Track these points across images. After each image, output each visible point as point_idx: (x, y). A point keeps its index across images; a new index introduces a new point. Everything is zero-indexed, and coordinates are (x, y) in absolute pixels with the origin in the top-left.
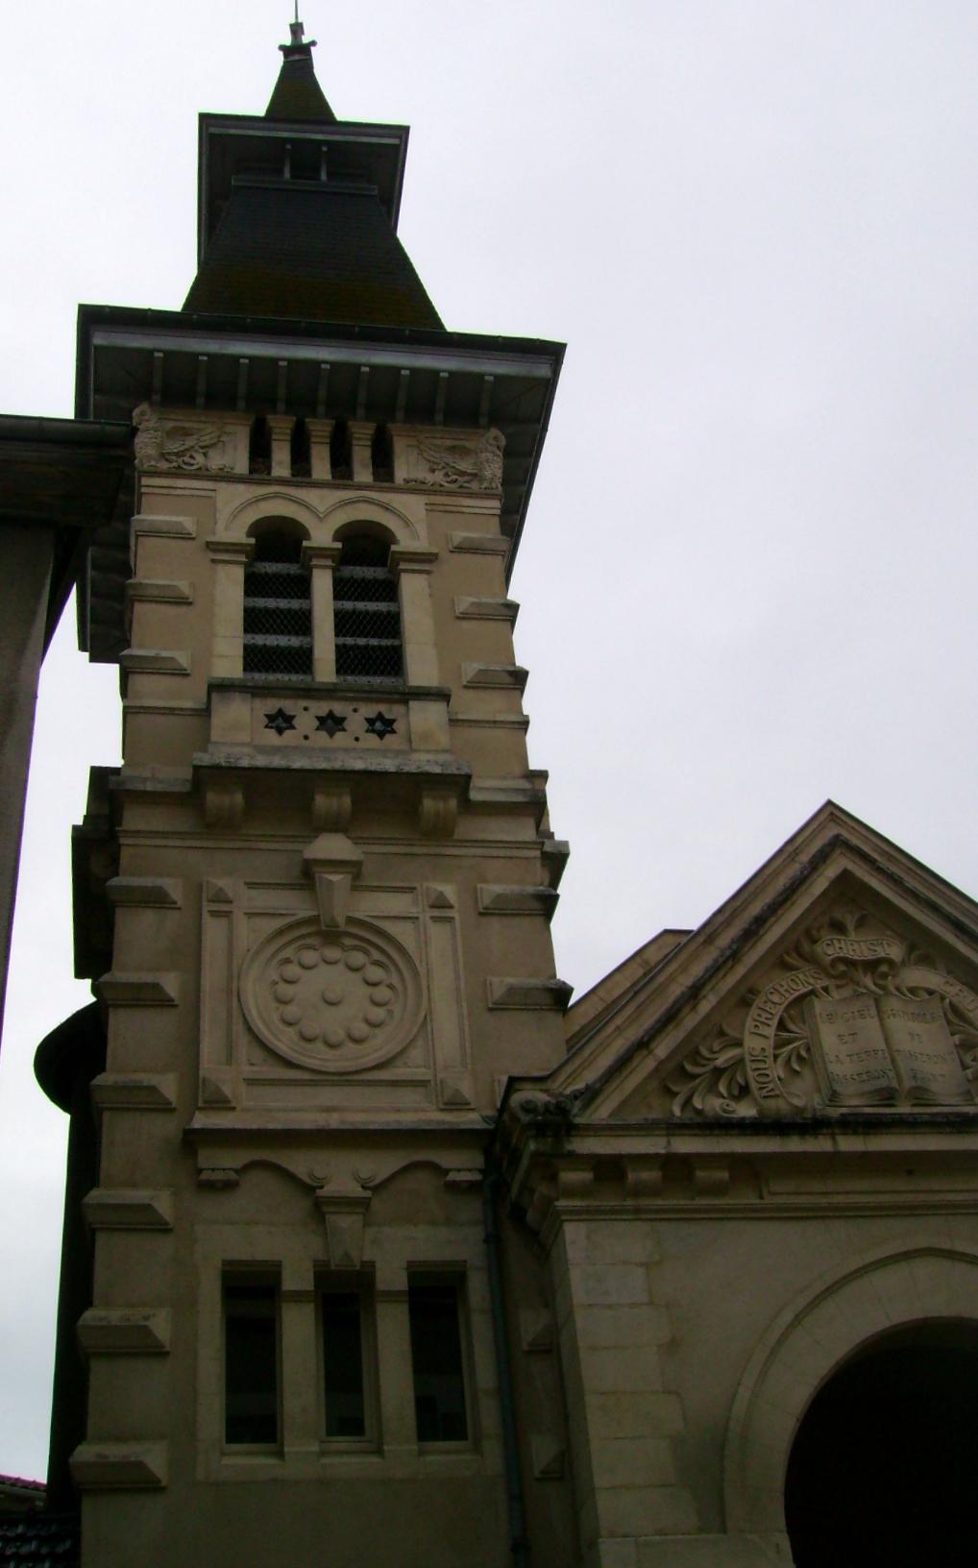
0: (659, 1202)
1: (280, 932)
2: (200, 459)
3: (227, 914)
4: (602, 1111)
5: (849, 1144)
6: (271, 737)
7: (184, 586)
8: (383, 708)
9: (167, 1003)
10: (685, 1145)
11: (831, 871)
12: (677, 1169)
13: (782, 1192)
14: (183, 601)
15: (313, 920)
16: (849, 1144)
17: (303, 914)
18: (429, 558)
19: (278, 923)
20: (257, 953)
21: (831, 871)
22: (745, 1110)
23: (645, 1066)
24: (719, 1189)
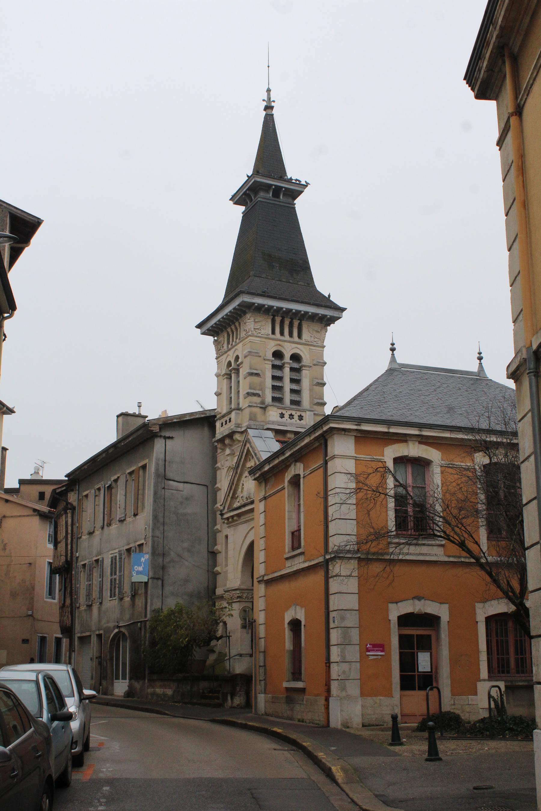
0: (233, 524)
1: (228, 470)
2: (221, 348)
3: (223, 469)
4: (226, 510)
5: (244, 509)
6: (222, 429)
7: (220, 391)
8: (229, 416)
9: (220, 489)
10: (232, 514)
11: (246, 448)
12: (232, 517)
13: (243, 519)
14: (220, 394)
15: (230, 467)
16: (244, 509)
17: (229, 466)
18: (242, 363)
19: (228, 468)
20: (226, 476)
21: (246, 448)
22: (239, 504)
23: (229, 499)
24: (237, 521)
